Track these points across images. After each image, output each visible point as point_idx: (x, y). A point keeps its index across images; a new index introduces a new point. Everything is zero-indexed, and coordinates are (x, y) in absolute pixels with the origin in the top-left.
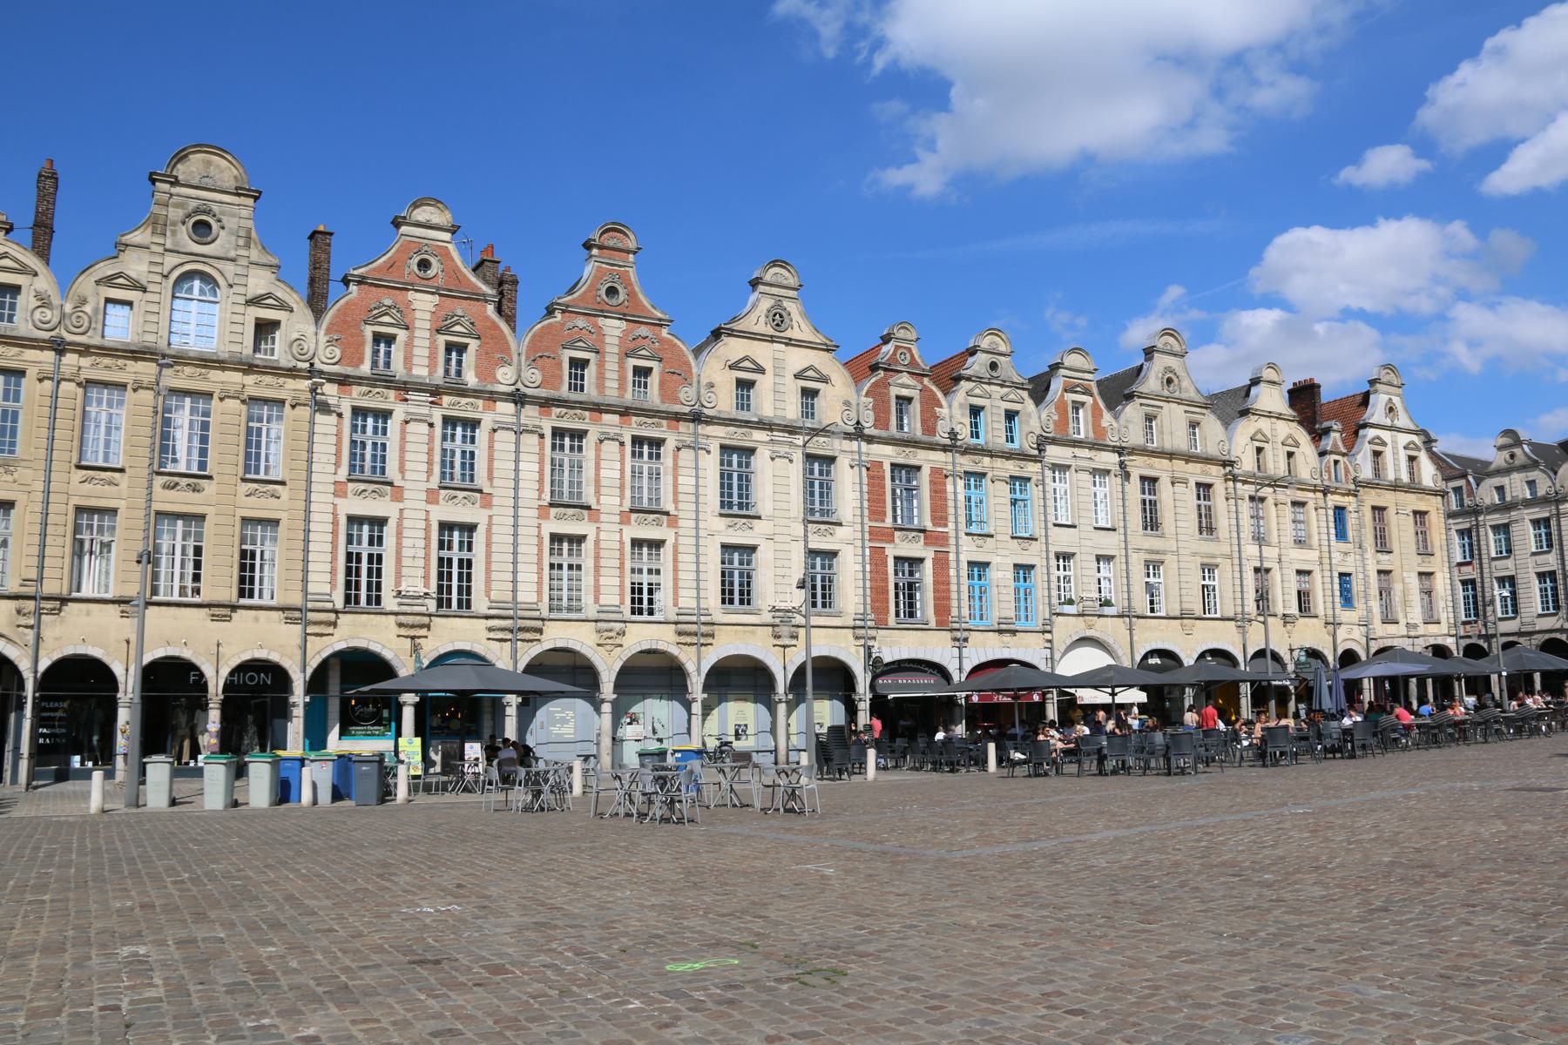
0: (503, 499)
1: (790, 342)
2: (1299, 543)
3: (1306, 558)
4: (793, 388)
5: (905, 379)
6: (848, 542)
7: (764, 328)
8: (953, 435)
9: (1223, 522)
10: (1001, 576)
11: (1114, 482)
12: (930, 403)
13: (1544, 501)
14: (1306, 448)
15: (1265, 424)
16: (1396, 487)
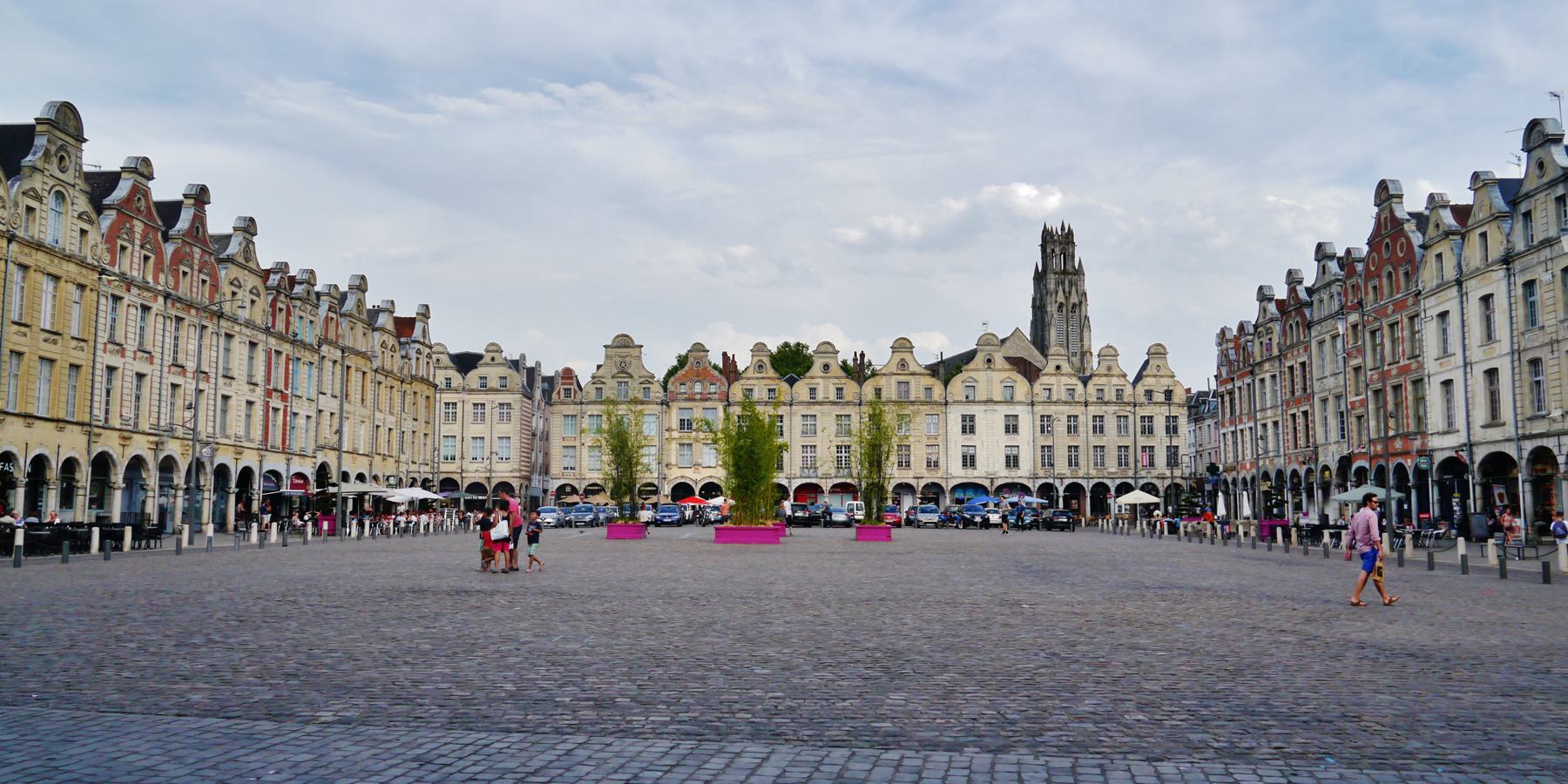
0: (157, 361)
1: (251, 271)
2: (392, 414)
3: (391, 421)
4: (248, 298)
5: (282, 298)
6: (258, 395)
7: (241, 260)
8: (295, 335)
9: (369, 397)
10: (301, 421)
11: (338, 367)
12: (289, 314)
13: (456, 391)
14: (397, 356)
15: (385, 337)
16: (424, 380)
